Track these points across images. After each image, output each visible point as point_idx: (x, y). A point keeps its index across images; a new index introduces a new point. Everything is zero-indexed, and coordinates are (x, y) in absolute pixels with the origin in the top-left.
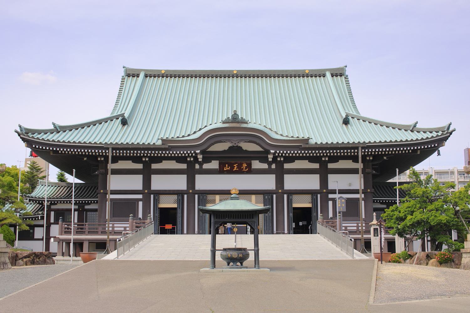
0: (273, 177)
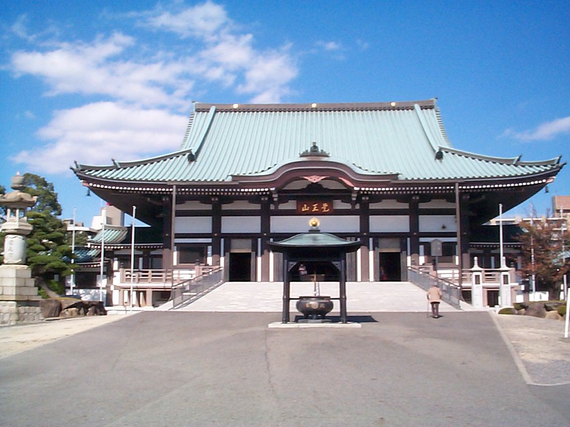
0: (356, 219)
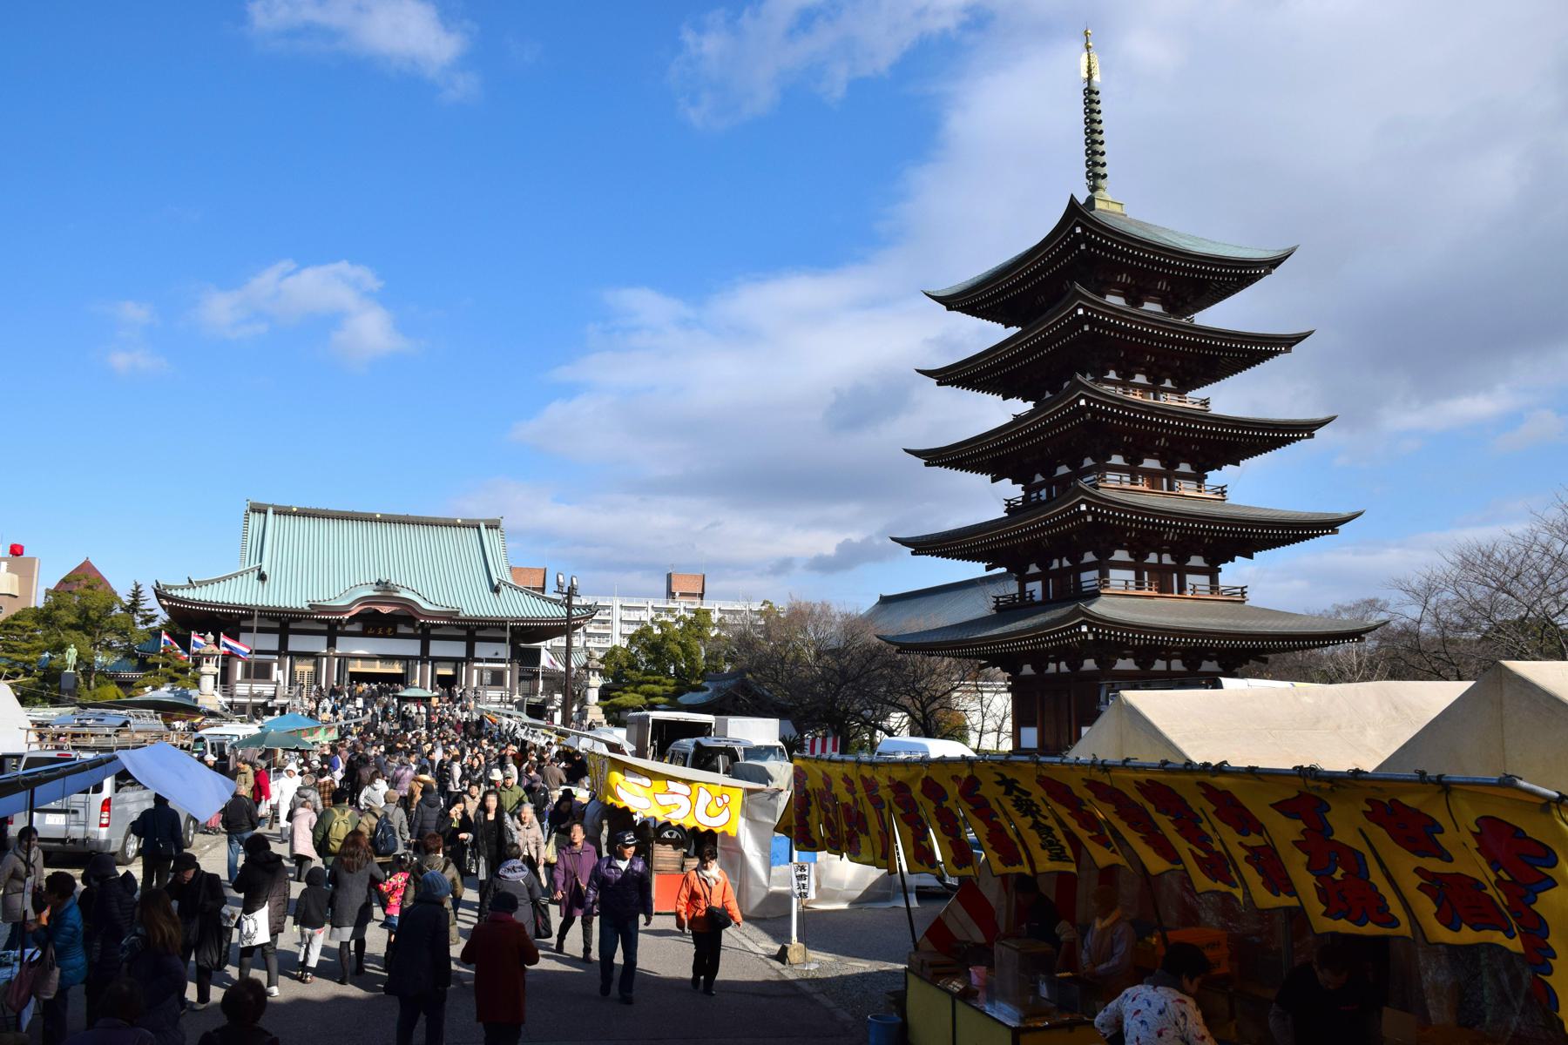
0: (418, 642)
